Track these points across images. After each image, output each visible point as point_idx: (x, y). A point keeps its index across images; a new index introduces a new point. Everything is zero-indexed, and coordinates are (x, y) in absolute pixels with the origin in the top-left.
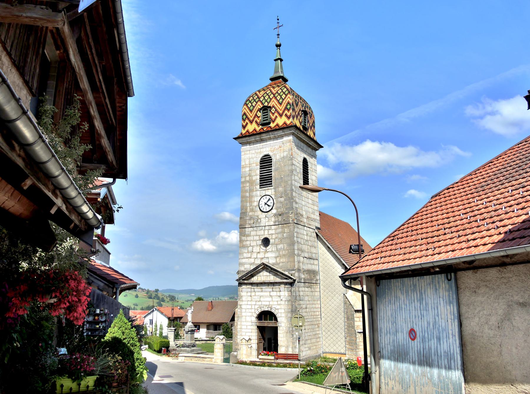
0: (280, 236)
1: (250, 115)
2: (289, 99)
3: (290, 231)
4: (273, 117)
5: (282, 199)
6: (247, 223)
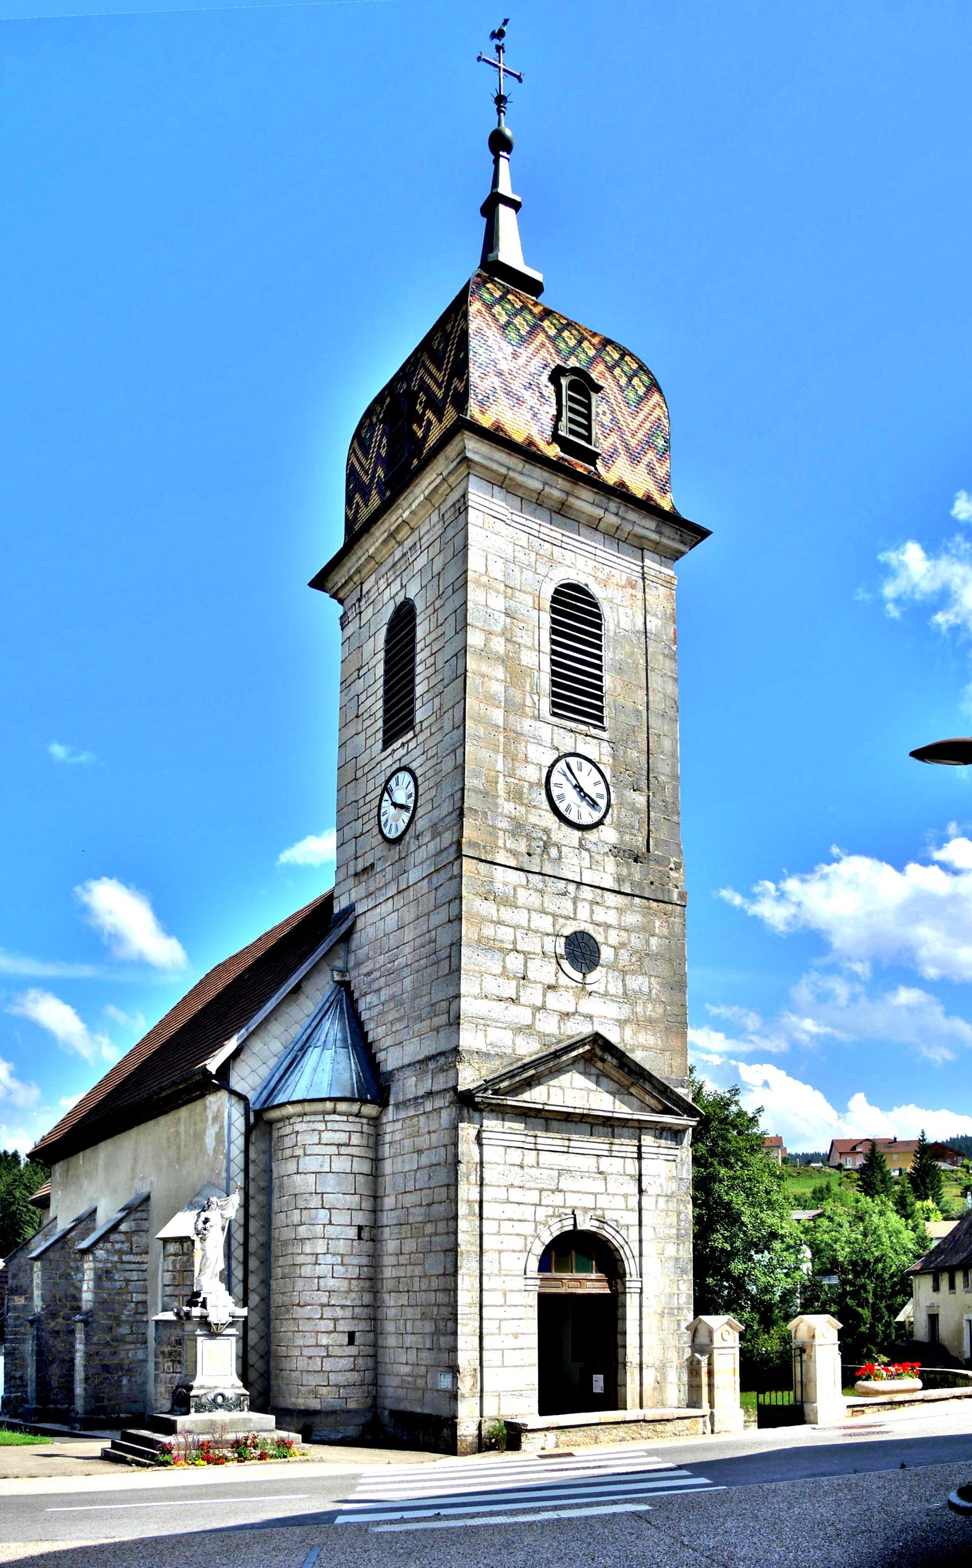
0: (636, 941)
6: (501, 843)
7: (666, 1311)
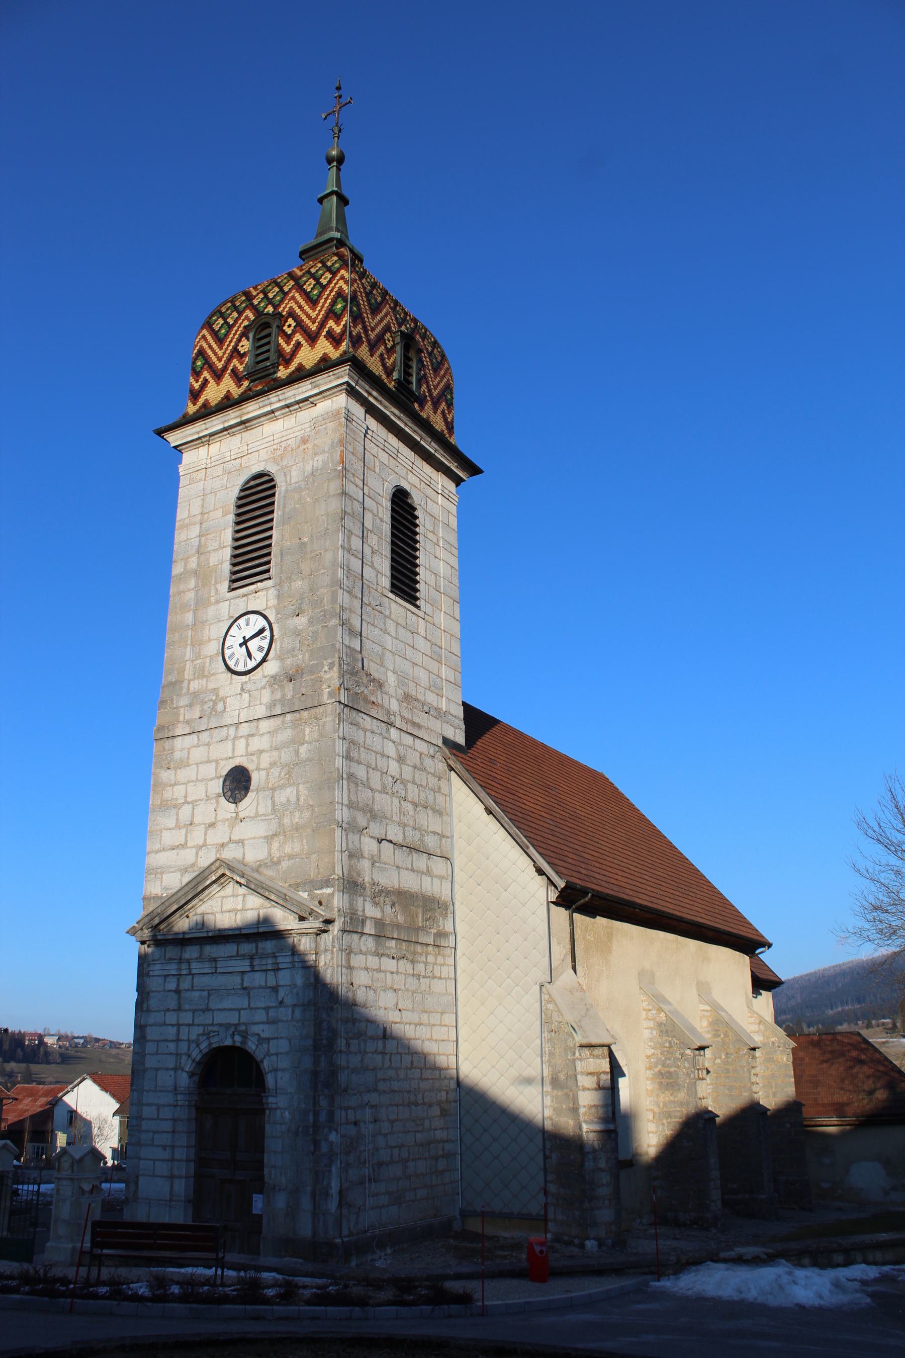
1: (215, 354)
2: (341, 283)
3: (321, 735)
4: (288, 349)
5: (301, 621)
6: (181, 719)
7: (300, 1129)
